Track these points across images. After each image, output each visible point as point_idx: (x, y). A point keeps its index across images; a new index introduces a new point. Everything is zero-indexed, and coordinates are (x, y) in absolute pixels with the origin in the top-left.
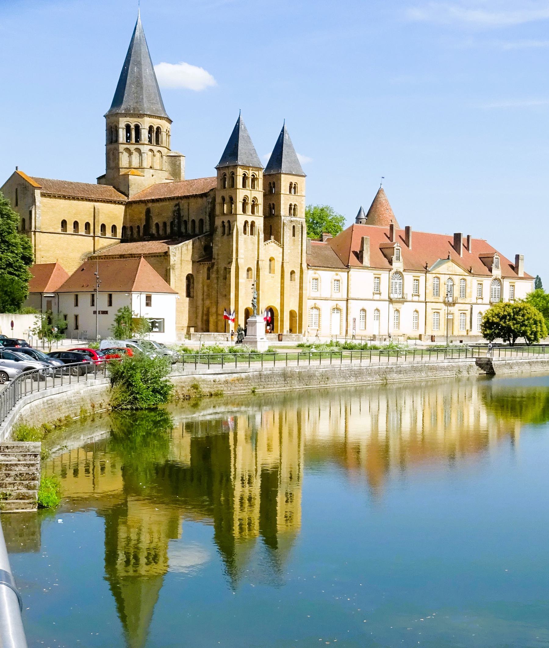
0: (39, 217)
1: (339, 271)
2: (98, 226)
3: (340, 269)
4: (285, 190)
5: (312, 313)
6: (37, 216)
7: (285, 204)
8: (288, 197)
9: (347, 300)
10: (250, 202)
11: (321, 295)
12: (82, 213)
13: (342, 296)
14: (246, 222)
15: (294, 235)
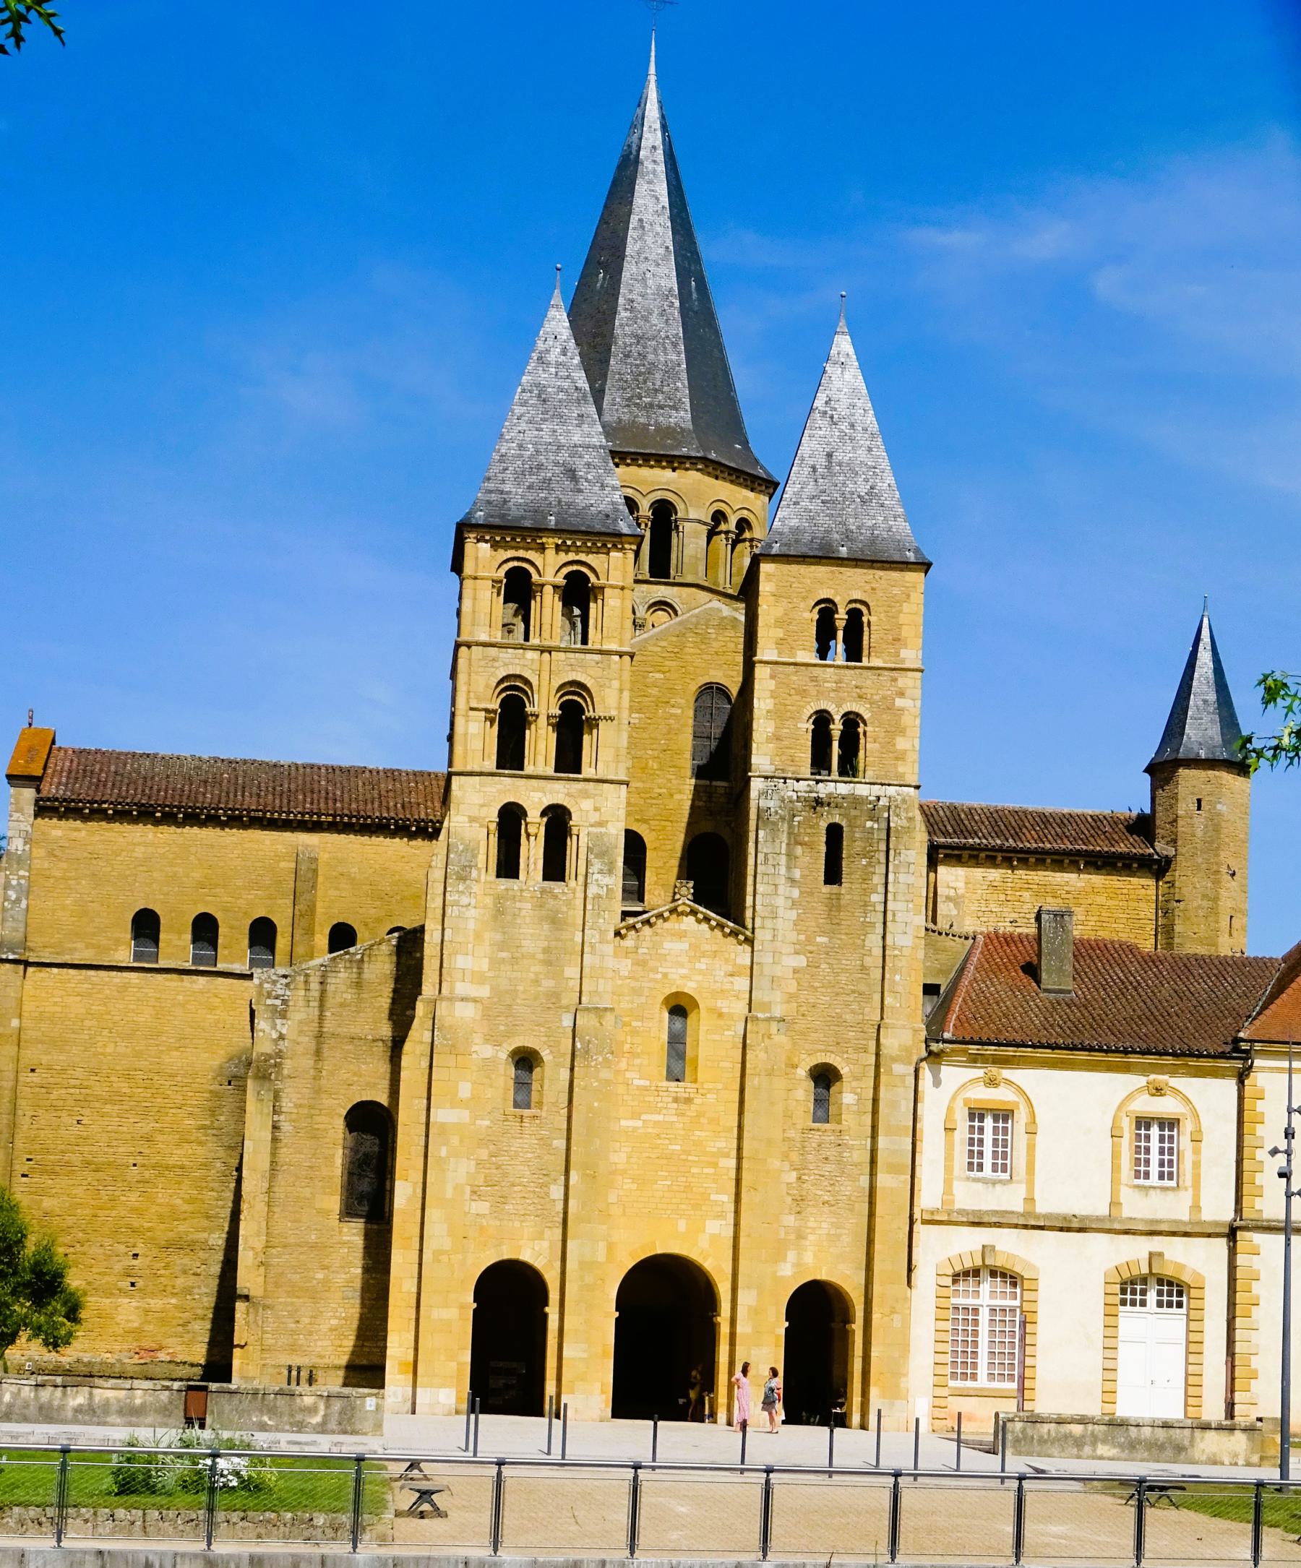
0: (18, 900)
1: (1173, 1071)
2: (310, 932)
3: (1170, 1060)
4: (780, 642)
5: (970, 1301)
6: (13, 895)
7: (779, 714)
8: (798, 678)
9: (1232, 1234)
10: (544, 705)
11: (1030, 1200)
12: (239, 883)
13: (1196, 1207)
14: (511, 818)
15: (833, 874)
